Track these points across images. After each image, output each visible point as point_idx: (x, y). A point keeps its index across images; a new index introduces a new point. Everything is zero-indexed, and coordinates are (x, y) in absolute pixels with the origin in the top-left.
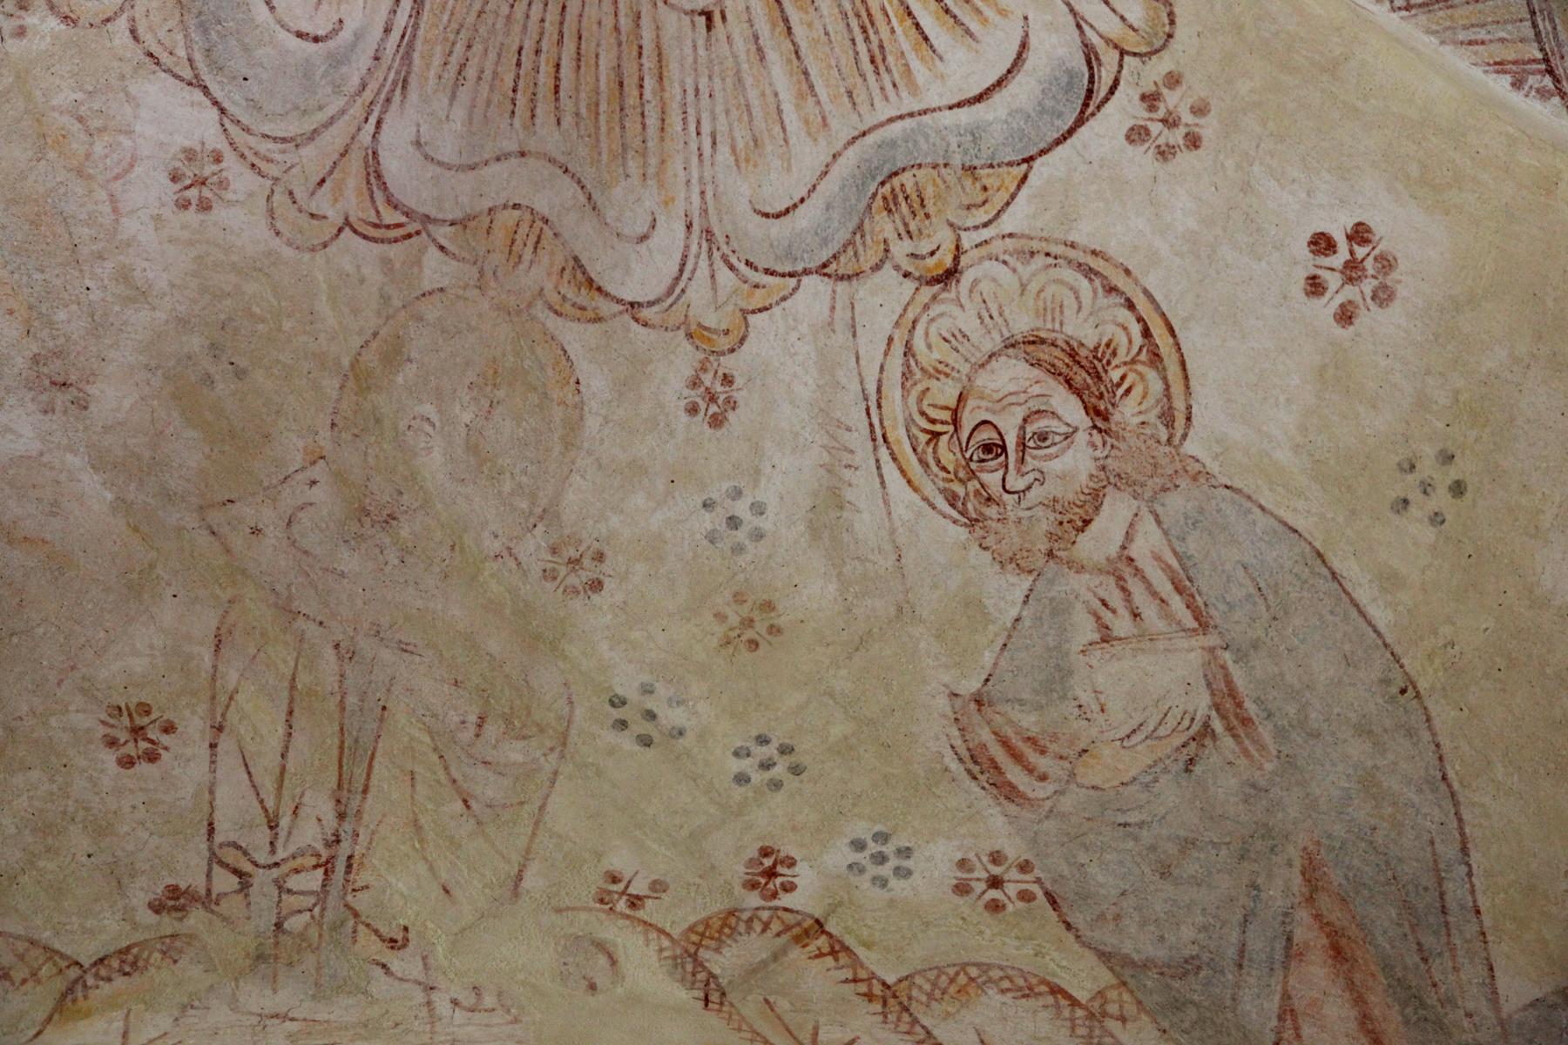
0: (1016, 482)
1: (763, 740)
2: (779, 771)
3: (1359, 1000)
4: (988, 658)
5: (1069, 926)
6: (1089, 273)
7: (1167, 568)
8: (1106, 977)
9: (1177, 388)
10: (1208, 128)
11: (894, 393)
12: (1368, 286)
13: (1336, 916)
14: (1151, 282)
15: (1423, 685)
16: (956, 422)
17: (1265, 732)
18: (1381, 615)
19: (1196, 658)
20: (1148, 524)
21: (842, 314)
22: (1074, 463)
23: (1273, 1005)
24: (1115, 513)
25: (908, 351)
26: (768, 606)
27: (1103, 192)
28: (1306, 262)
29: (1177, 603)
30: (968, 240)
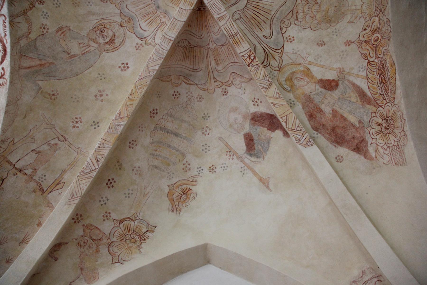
0: (98, 34)
1: (60, 4)
2: (56, 5)
3: (35, 66)
4: (75, 31)
5: (39, 36)
6: (123, 41)
7: (89, 50)
8: (33, 39)
9: (111, 51)
10: (138, 51)
11: (107, 21)
12: (123, 69)
13: (46, 65)
14: (122, 47)
15: (78, 76)
16: (105, 28)
17: (70, 60)
18: (86, 72)
19: (78, 53)
20: (94, 49)
21: (116, 15)
22: (101, 41)
23: (32, 57)
24: (96, 45)
25: (112, 22)
26: (78, 6)
27: (132, 41)
28: (125, 63)
29: (85, 51)
30: (125, 28)
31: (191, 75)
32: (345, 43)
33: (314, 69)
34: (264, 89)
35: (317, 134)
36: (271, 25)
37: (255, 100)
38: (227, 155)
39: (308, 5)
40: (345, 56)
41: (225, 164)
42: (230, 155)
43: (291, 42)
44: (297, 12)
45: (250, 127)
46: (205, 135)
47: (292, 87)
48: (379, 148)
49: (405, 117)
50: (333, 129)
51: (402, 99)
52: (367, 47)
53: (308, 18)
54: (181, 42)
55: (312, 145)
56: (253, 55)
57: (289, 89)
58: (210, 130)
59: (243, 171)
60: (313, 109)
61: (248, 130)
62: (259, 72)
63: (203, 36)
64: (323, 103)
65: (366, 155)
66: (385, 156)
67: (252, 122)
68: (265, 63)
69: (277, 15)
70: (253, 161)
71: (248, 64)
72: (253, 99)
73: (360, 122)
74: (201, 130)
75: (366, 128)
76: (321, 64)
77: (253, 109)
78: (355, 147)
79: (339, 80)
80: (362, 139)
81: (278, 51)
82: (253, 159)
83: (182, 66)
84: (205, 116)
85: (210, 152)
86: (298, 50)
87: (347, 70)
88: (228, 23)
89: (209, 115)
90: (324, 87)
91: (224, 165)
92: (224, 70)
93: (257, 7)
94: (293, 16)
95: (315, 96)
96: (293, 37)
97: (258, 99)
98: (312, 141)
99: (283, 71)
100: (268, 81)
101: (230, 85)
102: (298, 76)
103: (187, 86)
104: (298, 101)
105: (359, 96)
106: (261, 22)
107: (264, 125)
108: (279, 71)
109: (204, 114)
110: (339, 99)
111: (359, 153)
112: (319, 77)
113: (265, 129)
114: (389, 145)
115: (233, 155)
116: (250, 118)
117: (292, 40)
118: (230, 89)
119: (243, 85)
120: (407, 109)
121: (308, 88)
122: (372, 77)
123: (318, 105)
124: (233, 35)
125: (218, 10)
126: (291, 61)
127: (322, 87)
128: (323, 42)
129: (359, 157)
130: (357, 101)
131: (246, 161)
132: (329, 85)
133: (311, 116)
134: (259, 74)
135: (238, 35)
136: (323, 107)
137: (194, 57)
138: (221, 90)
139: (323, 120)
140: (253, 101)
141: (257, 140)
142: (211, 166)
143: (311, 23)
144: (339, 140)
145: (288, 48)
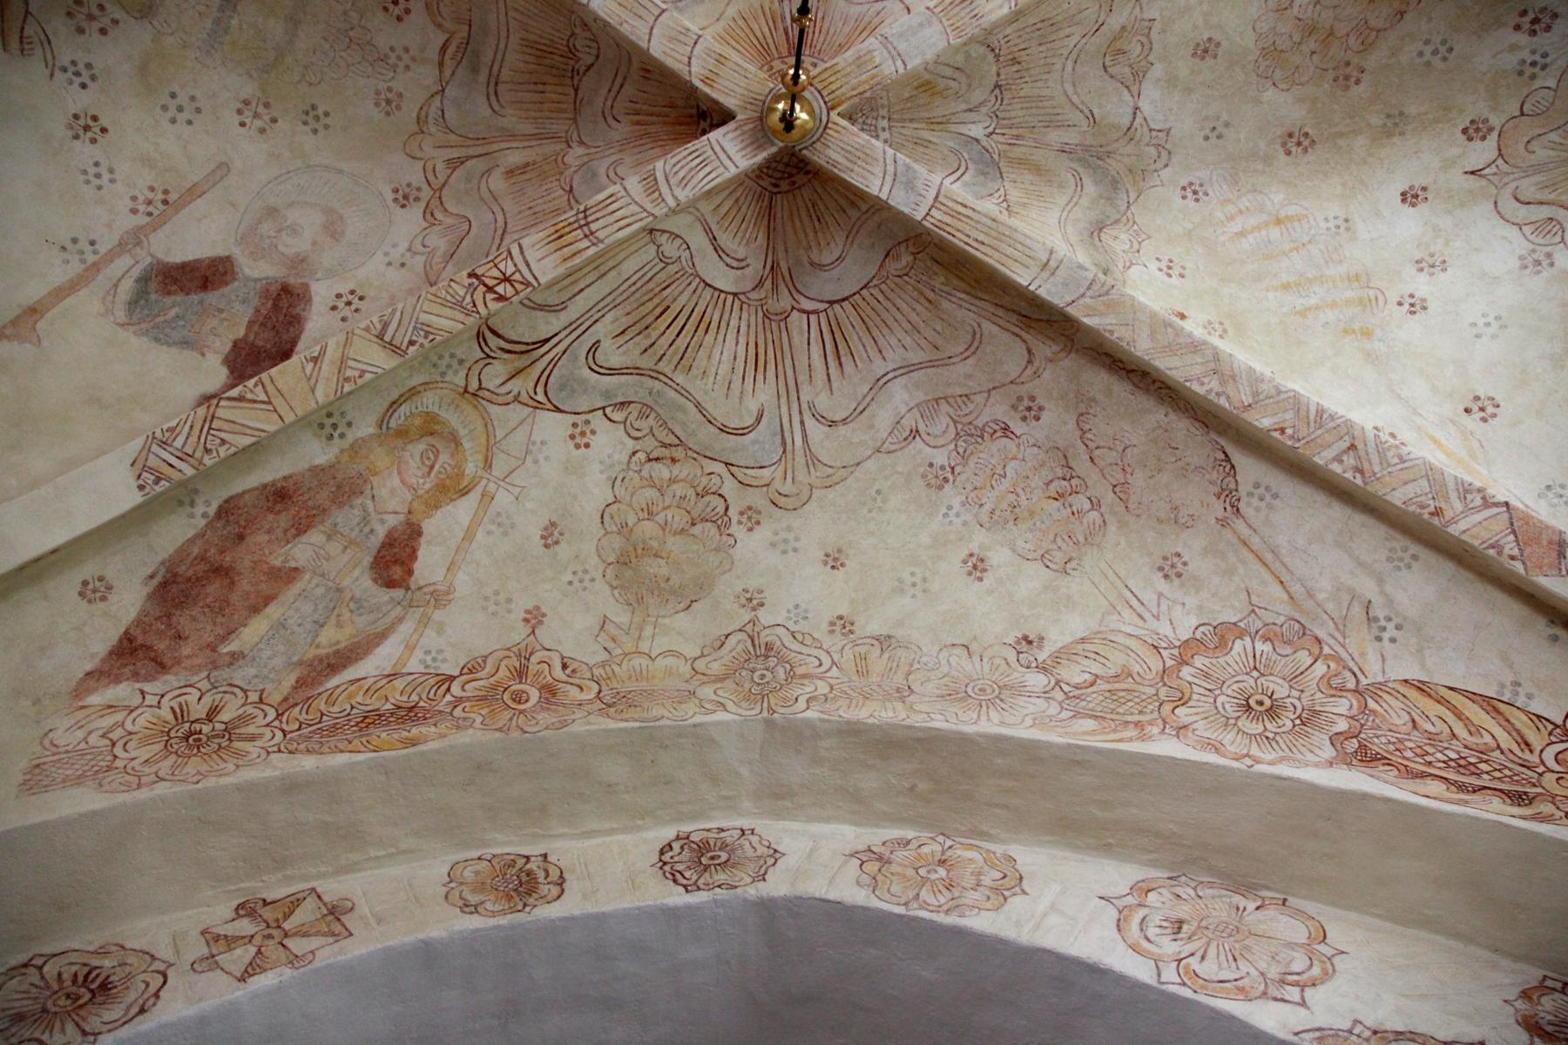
31: (475, 70)
32: (537, 608)
33: (461, 511)
34: (379, 326)
35: (204, 515)
36: (637, 371)
37: (356, 301)
38: (152, 189)
39: (693, 497)
40: (492, 608)
41: (112, 181)
42: (150, 203)
43: (572, 437)
44: (673, 460)
45: (256, 280)
46: (239, 112)
47: (402, 433)
48: (119, 717)
49: (211, 782)
50: (222, 572)
51: (277, 773)
52: (503, 672)
53: (651, 493)
54: (588, 35)
55: (141, 488)
56: (510, 291)
57: (393, 424)
58: (262, 131)
59: (77, 247)
60: (310, 503)
61: (247, 271)
62: (448, 312)
63: (613, 123)
64: (329, 538)
65: (101, 675)
66: (80, 734)
67: (274, 289)
68: (494, 342)
69: (672, 394)
70: (116, 286)
71: (479, 272)
72: (359, 293)
73: (235, 657)
74: (259, 94)
75: (208, 677)
76: (480, 535)
77: (322, 292)
78: (140, 640)
79: (408, 588)
80: (167, 660)
81: (540, 389)
82: (127, 285)
83: (503, 34)
84: (317, 118)
85: (166, 124)
86: (541, 457)
87: (438, 615)
88: (634, 208)
89: (322, 132)
90: (390, 542)
91: (106, 176)
92: (486, 195)
93: (703, 326)
94: (664, 445)
95: (356, 512)
96: (587, 446)
97: (356, 310)
98: (158, 489)
99: (464, 405)
100: (412, 343)
101: (428, 216)
102: (444, 457)
103: (433, 53)
104: (342, 451)
105: (337, 652)
106: (648, 336)
107: (256, 328)
108: (466, 391)
109: (327, 114)
110: (339, 590)
111: (111, 653)
112: (429, 526)
113: (241, 332)
114: (120, 744)
115: (150, 214)
116: (292, 281)
117: (578, 440)
118: (415, 213)
119: (420, 259)
120: (239, 788)
121: (392, 491)
122: (394, 689)
123: (323, 522)
124: (587, 224)
125: (681, 174)
126: (500, 434)
127: (389, 535)
128: (557, 543)
129: (92, 656)
130: (318, 646)
131: (123, 262)
132: (394, 560)
133: (279, 495)
134: (436, 309)
135: (586, 243)
136: (315, 537)
137: (540, 87)
138: (415, 184)
139: (262, 538)
140: (352, 292)
141: (201, 302)
142: (104, 122)
143: (630, 505)
144: (174, 589)
145: (552, 427)
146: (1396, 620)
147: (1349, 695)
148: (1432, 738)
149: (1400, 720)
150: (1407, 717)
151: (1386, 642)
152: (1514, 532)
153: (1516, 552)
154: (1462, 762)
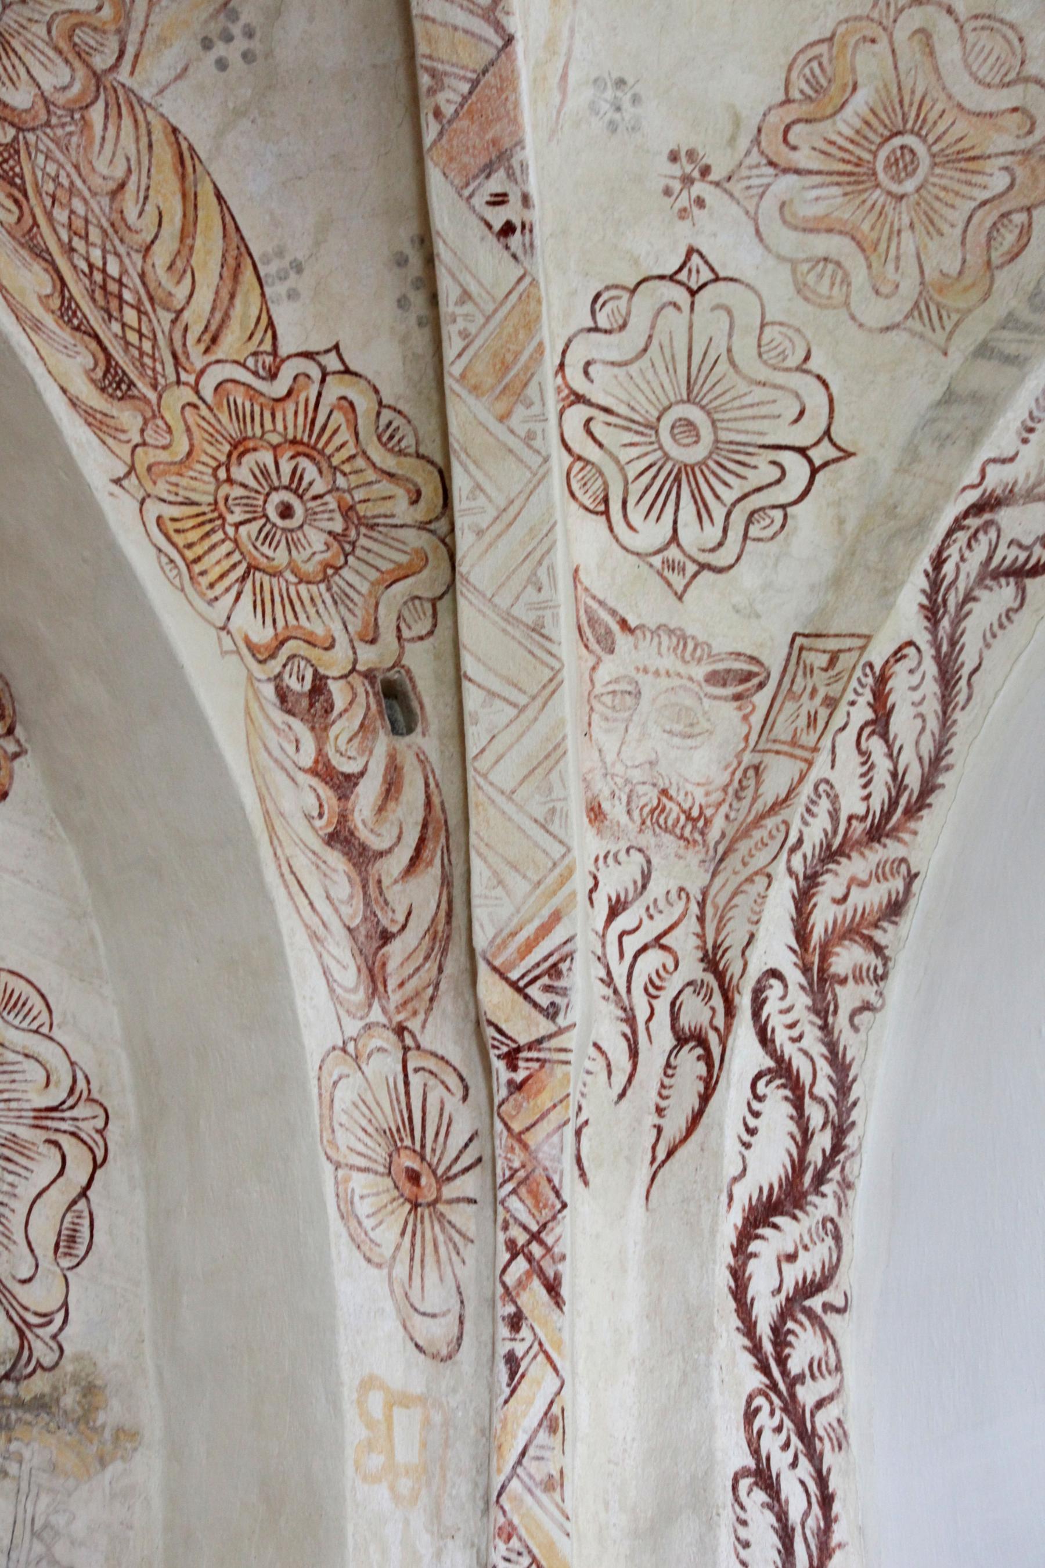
146: (256, 45)
147: (81, 72)
148: (118, 225)
149: (107, 167)
150: (119, 173)
151: (212, 56)
152: (475, 84)
153: (448, 110)
154: (113, 287)
